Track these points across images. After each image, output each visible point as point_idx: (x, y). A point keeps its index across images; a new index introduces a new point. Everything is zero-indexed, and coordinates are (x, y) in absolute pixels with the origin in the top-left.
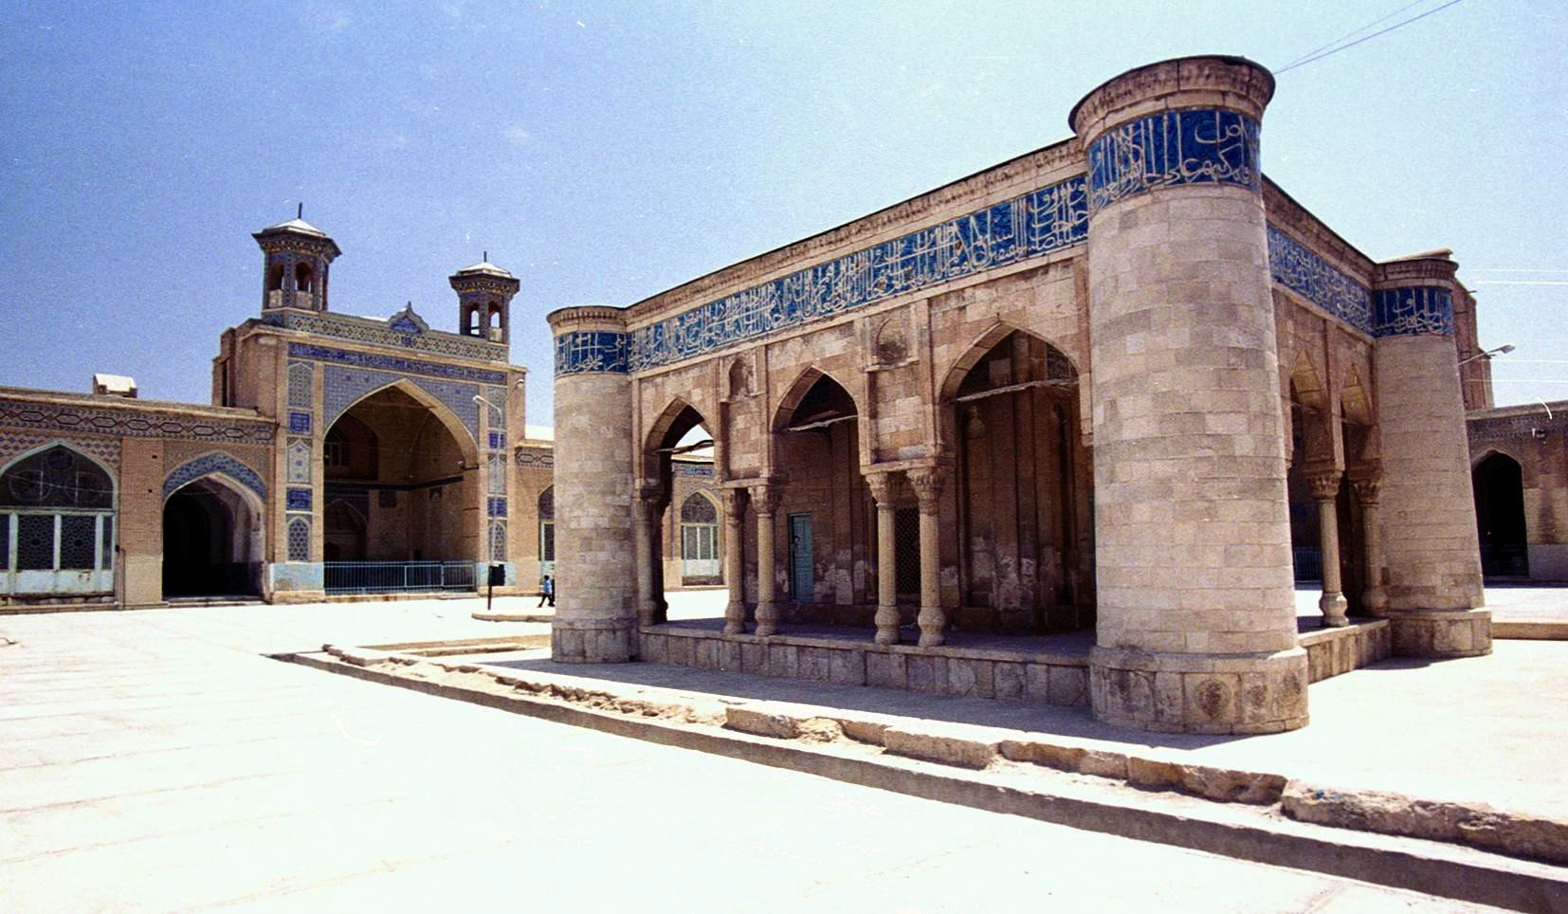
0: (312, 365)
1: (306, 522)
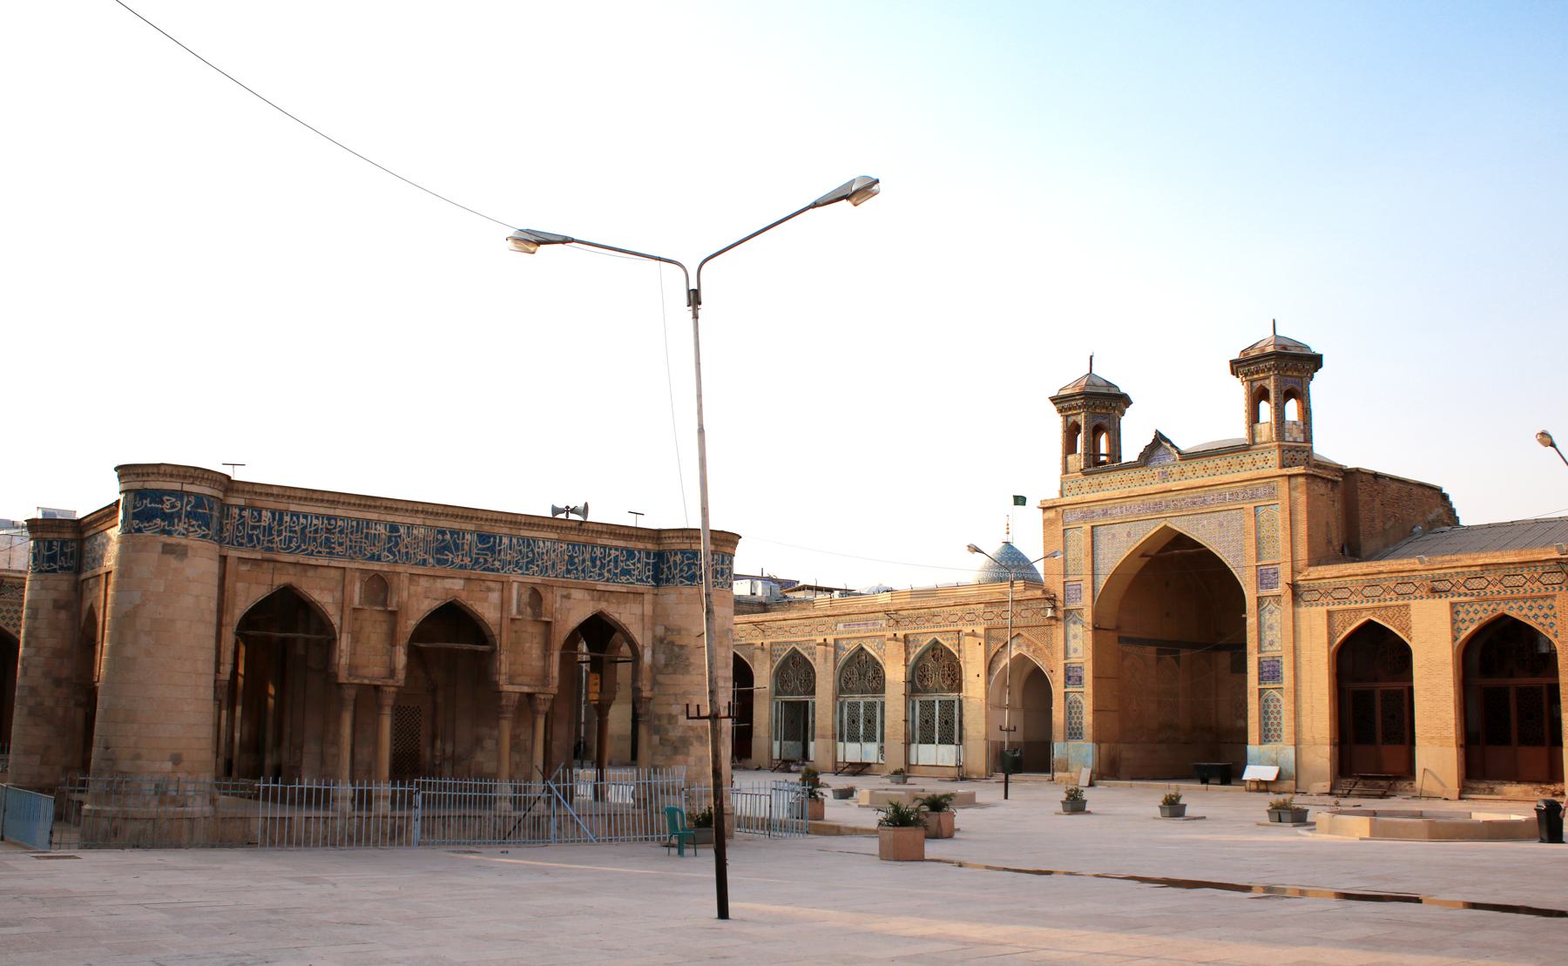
1: (1080, 698)
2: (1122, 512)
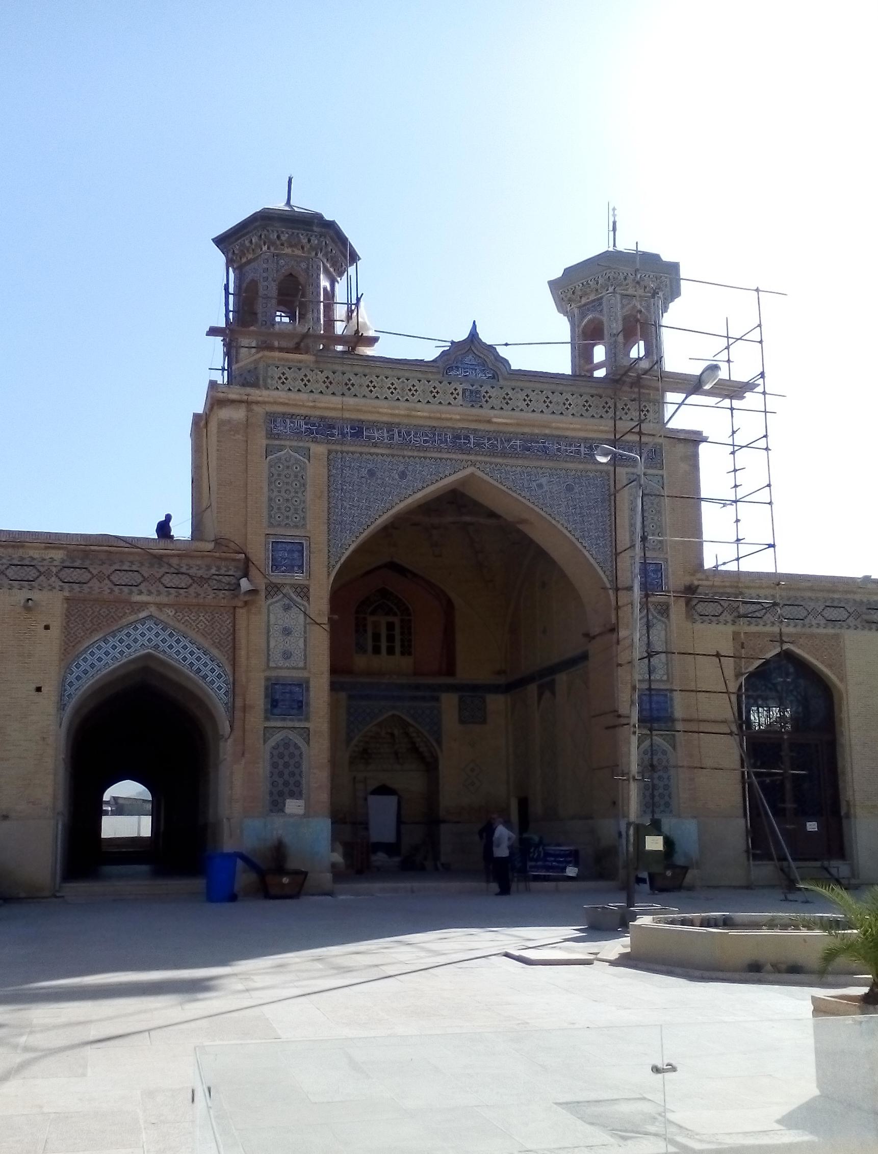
0: (307, 454)
2: (392, 438)
